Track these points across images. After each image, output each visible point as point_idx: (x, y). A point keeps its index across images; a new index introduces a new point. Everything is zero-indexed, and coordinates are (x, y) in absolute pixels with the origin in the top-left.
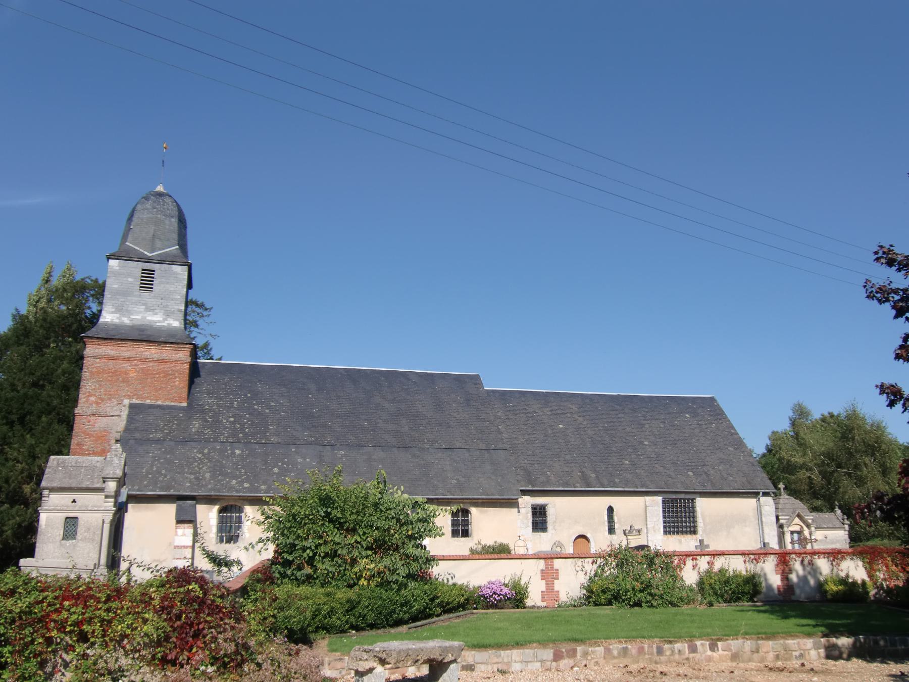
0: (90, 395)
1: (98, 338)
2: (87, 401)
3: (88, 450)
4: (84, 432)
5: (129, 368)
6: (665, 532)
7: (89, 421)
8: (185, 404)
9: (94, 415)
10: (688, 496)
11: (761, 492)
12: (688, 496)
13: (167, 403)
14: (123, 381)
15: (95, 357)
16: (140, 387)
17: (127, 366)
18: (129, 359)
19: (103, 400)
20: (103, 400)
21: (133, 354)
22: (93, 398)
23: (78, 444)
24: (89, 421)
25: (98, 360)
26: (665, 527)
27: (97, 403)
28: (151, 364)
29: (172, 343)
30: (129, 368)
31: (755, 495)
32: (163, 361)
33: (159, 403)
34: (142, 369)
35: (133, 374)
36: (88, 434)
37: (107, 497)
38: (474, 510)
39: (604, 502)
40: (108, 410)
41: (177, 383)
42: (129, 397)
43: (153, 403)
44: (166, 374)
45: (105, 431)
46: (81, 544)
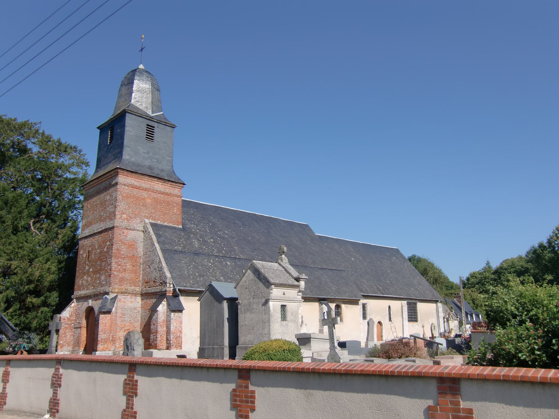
0: (123, 213)
1: (128, 171)
2: (121, 217)
3: (123, 255)
4: (121, 241)
5: (146, 196)
6: (409, 321)
7: (123, 233)
8: (181, 227)
9: (127, 229)
10: (413, 301)
11: (439, 300)
12: (413, 301)
13: (170, 225)
14: (143, 206)
15: (125, 185)
16: (153, 211)
17: (145, 194)
18: (146, 190)
19: (131, 218)
20: (131, 218)
21: (148, 186)
22: (124, 216)
23: (117, 250)
24: (123, 233)
25: (127, 187)
26: (409, 318)
27: (128, 220)
28: (160, 195)
29: (173, 182)
30: (146, 196)
31: (436, 302)
32: (167, 194)
33: (166, 224)
34: (154, 198)
35: (148, 201)
36: (123, 243)
37: (299, 292)
38: (343, 306)
39: (385, 303)
40: (135, 226)
41: (175, 211)
42: (148, 218)
43: (162, 223)
44: (168, 203)
45: (134, 241)
46: (290, 324)
